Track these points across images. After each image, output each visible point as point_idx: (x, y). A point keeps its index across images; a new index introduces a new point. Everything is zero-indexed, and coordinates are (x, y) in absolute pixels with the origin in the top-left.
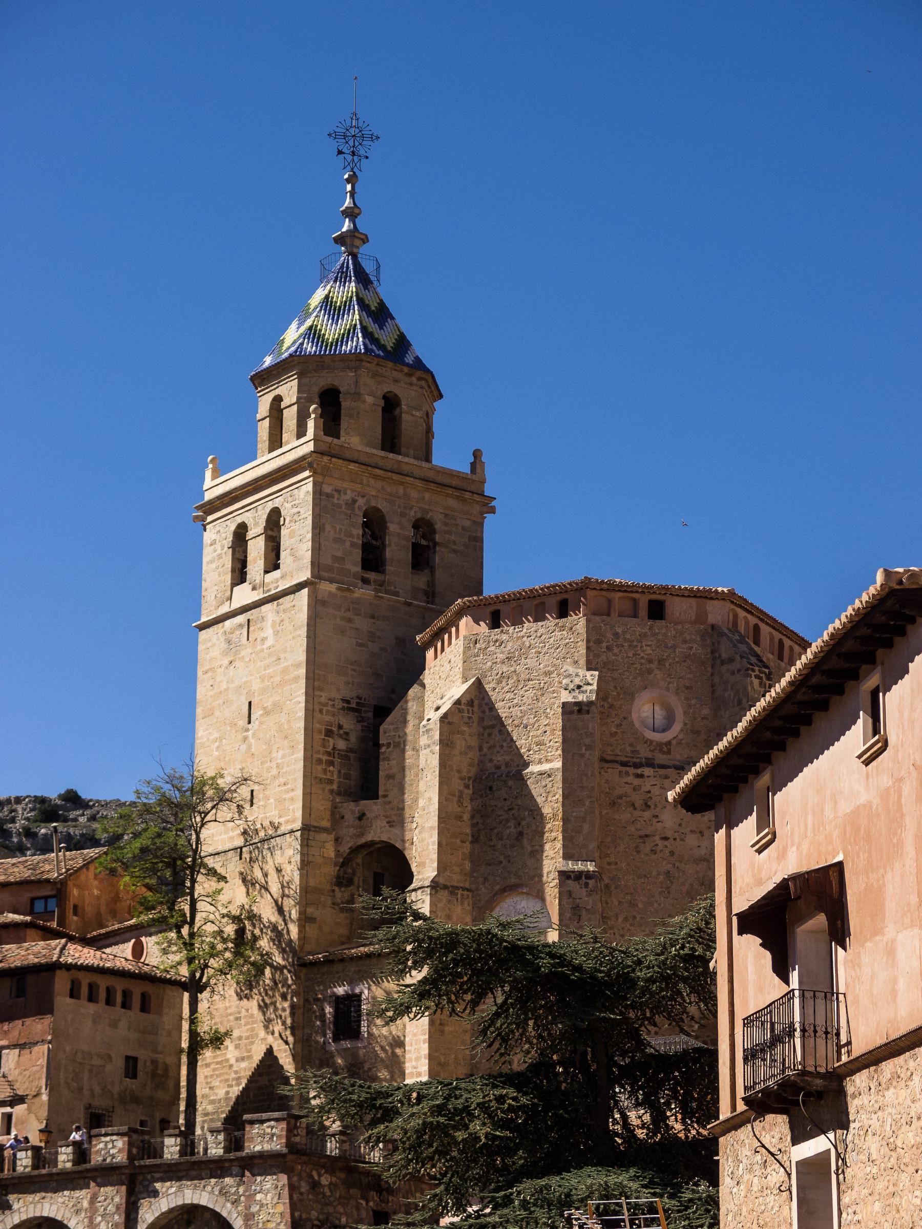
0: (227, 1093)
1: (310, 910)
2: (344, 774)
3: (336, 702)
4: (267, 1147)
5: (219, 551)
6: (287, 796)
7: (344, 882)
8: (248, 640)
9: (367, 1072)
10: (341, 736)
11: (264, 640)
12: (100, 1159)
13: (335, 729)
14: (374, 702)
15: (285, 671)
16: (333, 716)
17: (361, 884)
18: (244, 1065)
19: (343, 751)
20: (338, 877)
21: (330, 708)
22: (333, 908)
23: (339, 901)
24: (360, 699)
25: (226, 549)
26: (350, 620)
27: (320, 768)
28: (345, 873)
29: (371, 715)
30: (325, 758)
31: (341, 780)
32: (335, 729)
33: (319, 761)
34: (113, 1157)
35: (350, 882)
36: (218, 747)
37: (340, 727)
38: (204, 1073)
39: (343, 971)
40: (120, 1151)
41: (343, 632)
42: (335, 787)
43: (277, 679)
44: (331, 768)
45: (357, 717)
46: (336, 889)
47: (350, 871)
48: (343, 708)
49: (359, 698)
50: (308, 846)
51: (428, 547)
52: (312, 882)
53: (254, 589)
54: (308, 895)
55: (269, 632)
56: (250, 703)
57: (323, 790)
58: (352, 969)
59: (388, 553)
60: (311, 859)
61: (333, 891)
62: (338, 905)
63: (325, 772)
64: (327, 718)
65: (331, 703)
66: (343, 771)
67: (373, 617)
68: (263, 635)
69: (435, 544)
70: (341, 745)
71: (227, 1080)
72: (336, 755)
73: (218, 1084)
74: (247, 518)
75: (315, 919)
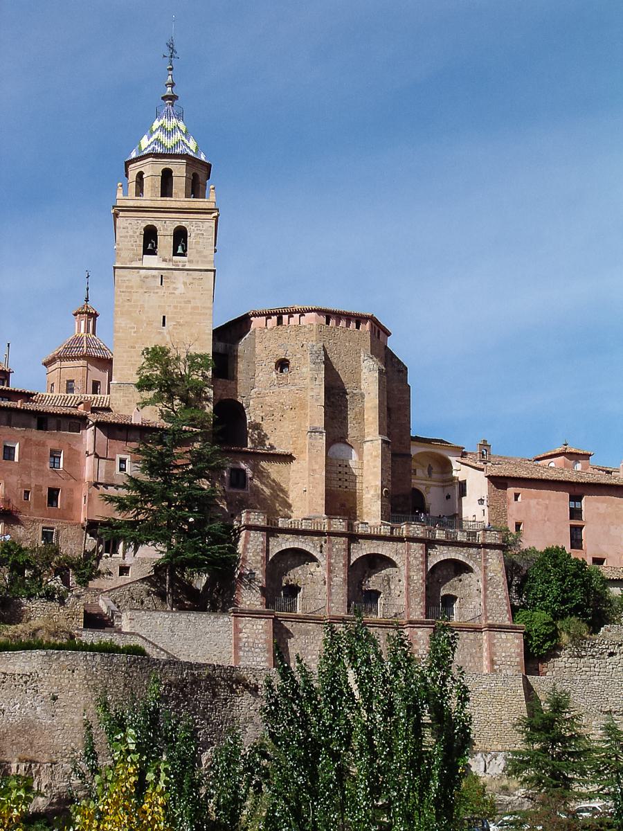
4: (493, 542)
5: (131, 233)
8: (161, 284)
11: (175, 289)
12: (412, 534)
15: (194, 308)
25: (138, 234)
34: (418, 534)
36: (135, 332)
40: (422, 532)
43: (190, 310)
53: (164, 260)
55: (181, 288)
56: (164, 317)
68: (174, 286)
74: (158, 224)
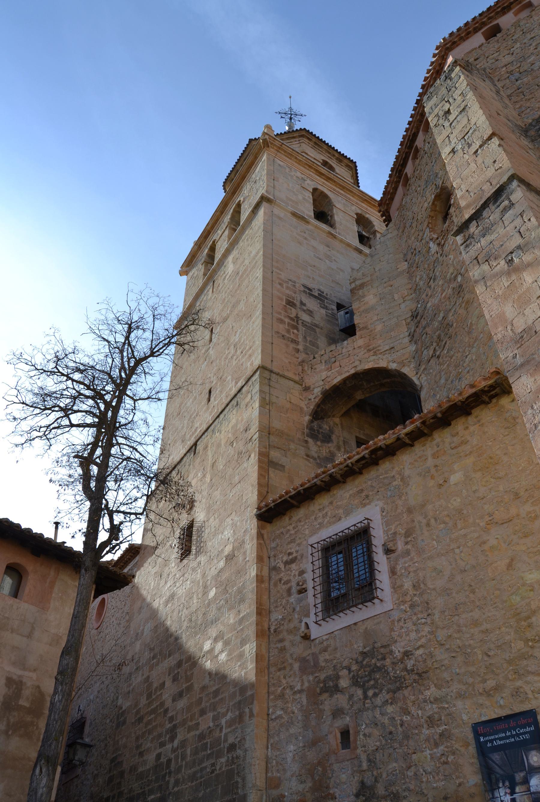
0: (159, 756)
1: (275, 454)
2: (310, 341)
3: (297, 285)
6: (244, 360)
7: (320, 436)
9: (402, 661)
10: (304, 311)
13: (298, 304)
14: (336, 300)
16: (295, 293)
17: (341, 443)
18: (182, 704)
19: (308, 323)
20: (311, 429)
21: (289, 286)
22: (308, 460)
23: (316, 455)
24: (323, 293)
26: (306, 239)
27: (281, 326)
28: (321, 428)
29: (335, 307)
30: (287, 320)
31: (308, 345)
32: (298, 304)
33: (281, 321)
35: (327, 439)
37: (302, 303)
38: (135, 733)
39: (331, 503)
41: (300, 243)
42: (300, 347)
44: (295, 331)
45: (320, 303)
46: (310, 440)
47: (326, 427)
48: (304, 291)
49: (319, 290)
50: (270, 386)
51: (368, 238)
52: (277, 424)
54: (272, 438)
57: (287, 346)
58: (347, 495)
59: (336, 218)
60: (274, 399)
61: (306, 442)
62: (313, 458)
63: (288, 331)
64: (288, 292)
65: (290, 283)
66: (308, 339)
67: (328, 246)
69: (375, 233)
70: (305, 317)
71: (160, 736)
72: (301, 324)
73: (149, 745)
75: (283, 467)
